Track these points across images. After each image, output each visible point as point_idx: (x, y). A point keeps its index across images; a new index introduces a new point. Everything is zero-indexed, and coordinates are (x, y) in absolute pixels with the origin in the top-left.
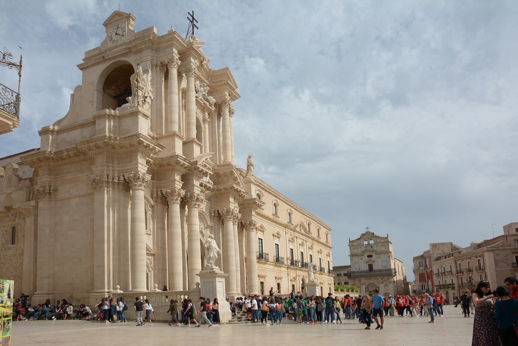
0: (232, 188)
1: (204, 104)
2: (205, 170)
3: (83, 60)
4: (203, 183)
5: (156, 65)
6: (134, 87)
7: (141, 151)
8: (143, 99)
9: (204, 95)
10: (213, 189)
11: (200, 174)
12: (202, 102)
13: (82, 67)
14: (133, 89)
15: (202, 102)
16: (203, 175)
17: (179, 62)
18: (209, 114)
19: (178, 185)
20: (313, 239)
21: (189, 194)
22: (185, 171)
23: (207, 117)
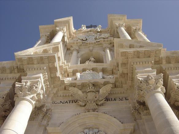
11: (35, 66)
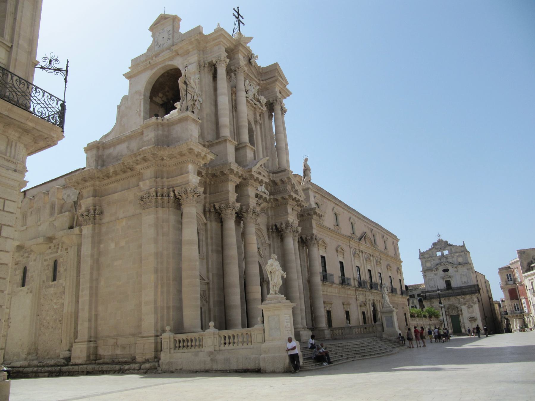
0: (290, 196)
1: (255, 104)
2: (261, 177)
3: (129, 68)
4: (258, 193)
5: (204, 66)
6: (182, 91)
7: (192, 161)
8: (193, 103)
9: (254, 95)
10: (270, 199)
12: (252, 103)
13: (128, 76)
14: (182, 93)
15: (252, 103)
16: (258, 184)
17: (228, 60)
18: (260, 115)
19: (233, 197)
20: (381, 252)
21: (244, 207)
22: (238, 181)
23: (258, 118)
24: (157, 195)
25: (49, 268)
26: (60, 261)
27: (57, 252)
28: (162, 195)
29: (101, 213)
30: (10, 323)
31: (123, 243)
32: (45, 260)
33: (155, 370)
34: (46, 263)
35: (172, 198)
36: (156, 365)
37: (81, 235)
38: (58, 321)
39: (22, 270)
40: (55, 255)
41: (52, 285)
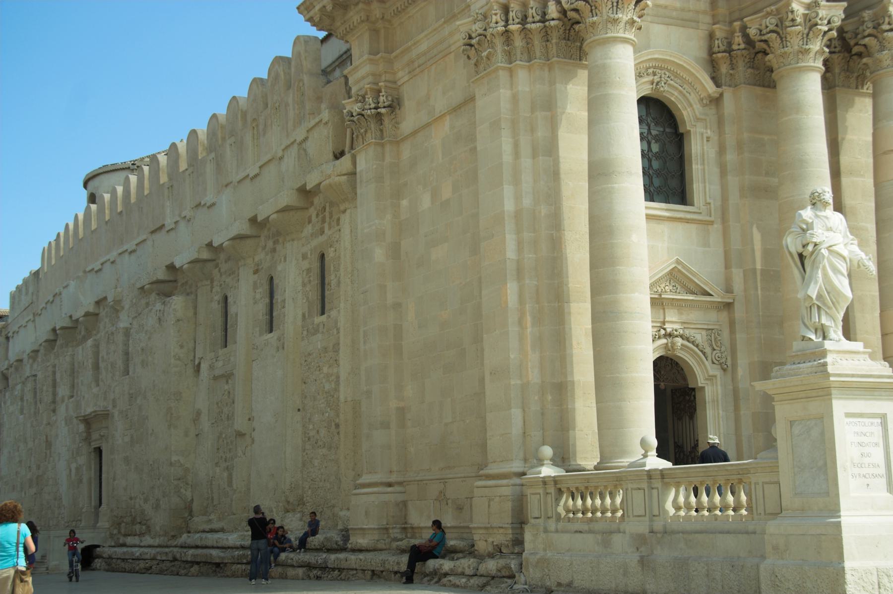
24: (507, 21)
25: (311, 279)
26: (330, 254)
27: (322, 232)
28: (524, 20)
29: (395, 105)
30: (254, 430)
31: (446, 193)
32: (304, 257)
33: (509, 581)
34: (305, 265)
35: (552, 23)
36: (513, 566)
37: (355, 174)
38: (333, 427)
39: (266, 287)
40: (322, 239)
41: (318, 325)
